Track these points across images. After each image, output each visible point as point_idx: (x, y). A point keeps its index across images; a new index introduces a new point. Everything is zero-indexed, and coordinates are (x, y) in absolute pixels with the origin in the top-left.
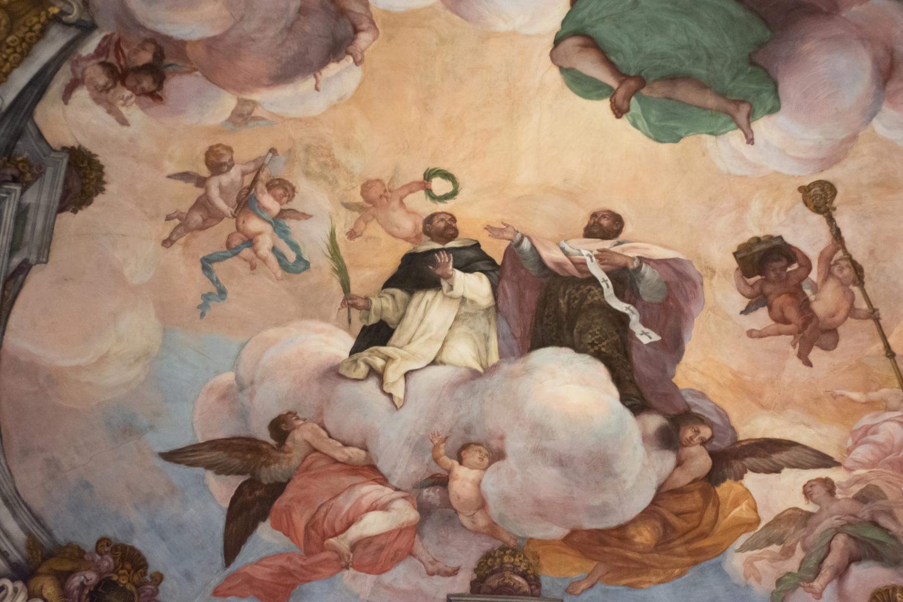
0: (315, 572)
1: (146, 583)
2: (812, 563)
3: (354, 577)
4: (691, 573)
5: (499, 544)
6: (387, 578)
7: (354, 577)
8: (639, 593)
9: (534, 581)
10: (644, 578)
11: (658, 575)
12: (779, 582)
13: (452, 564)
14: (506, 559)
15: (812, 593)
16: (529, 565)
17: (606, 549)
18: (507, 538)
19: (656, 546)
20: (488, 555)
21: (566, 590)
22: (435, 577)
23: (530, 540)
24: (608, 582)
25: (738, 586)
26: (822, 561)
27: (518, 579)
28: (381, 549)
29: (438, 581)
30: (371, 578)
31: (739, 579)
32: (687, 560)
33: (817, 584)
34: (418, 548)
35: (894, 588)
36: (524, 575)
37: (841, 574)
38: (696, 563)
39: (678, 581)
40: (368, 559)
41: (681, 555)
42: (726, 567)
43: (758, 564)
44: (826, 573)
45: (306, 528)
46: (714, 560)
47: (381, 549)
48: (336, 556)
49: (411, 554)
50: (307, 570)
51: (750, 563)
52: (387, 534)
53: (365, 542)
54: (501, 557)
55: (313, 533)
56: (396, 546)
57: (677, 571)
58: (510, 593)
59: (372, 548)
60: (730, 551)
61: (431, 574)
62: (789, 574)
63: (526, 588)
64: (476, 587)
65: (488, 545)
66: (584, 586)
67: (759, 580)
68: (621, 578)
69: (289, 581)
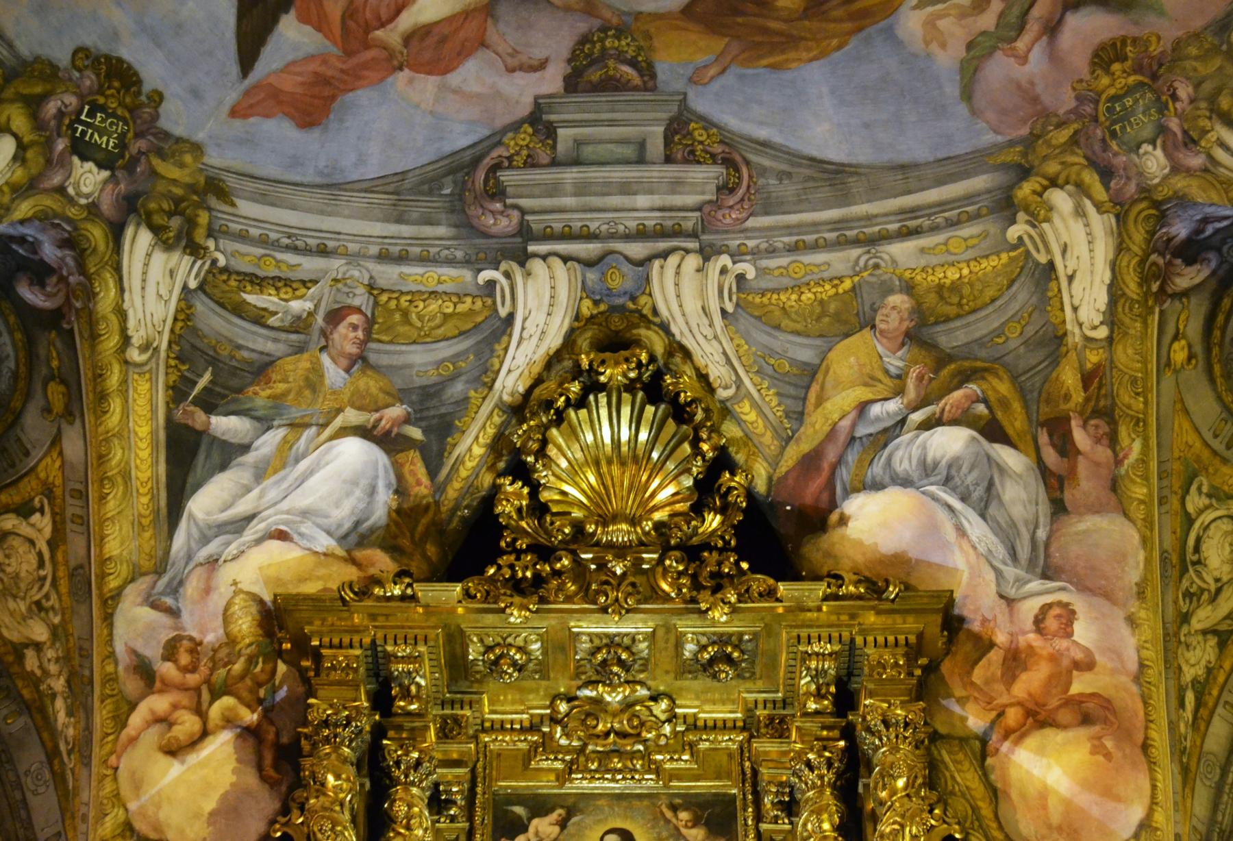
0: (359, 78)
1: (142, 105)
2: (1013, 17)
3: (411, 81)
4: (854, 42)
5: (597, 23)
6: (454, 79)
7: (411, 81)
8: (787, 75)
9: (648, 71)
10: (792, 55)
11: (809, 50)
12: (970, 46)
13: (538, 54)
14: (608, 43)
15: (1015, 57)
16: (640, 48)
17: (740, 20)
18: (607, 14)
19: (806, 9)
20: (584, 40)
21: (690, 80)
22: (518, 74)
23: (638, 15)
24: (747, 63)
25: (915, 56)
26: (1026, 12)
27: (626, 69)
28: (443, 40)
29: (520, 78)
30: (432, 79)
31: (918, 46)
32: (848, 26)
33: (1021, 45)
34: (492, 35)
35: (1124, 41)
36: (633, 63)
37: (1052, 29)
38: (860, 29)
39: (837, 55)
40: (427, 55)
41: (835, 21)
42: (900, 33)
43: (942, 24)
44: (1033, 28)
45: (343, 17)
46: (882, 24)
47: (443, 40)
48: (384, 54)
49: (483, 44)
50: (348, 75)
51: (930, 23)
52: (449, 20)
53: (421, 33)
54: (602, 41)
55: (352, 24)
56: (462, 35)
57: (835, 42)
58: (616, 89)
59: (430, 41)
60: (903, 9)
61: (511, 70)
62: (983, 33)
63: (637, 81)
64: (572, 84)
65: (582, 26)
66: (712, 71)
67: (943, 46)
68: (761, 57)
69: (327, 92)
